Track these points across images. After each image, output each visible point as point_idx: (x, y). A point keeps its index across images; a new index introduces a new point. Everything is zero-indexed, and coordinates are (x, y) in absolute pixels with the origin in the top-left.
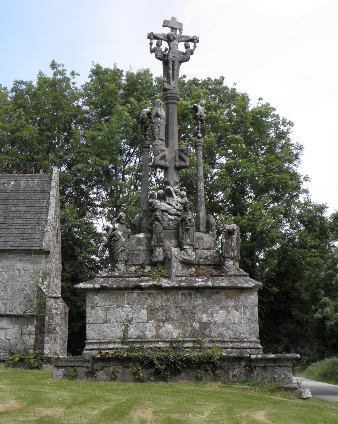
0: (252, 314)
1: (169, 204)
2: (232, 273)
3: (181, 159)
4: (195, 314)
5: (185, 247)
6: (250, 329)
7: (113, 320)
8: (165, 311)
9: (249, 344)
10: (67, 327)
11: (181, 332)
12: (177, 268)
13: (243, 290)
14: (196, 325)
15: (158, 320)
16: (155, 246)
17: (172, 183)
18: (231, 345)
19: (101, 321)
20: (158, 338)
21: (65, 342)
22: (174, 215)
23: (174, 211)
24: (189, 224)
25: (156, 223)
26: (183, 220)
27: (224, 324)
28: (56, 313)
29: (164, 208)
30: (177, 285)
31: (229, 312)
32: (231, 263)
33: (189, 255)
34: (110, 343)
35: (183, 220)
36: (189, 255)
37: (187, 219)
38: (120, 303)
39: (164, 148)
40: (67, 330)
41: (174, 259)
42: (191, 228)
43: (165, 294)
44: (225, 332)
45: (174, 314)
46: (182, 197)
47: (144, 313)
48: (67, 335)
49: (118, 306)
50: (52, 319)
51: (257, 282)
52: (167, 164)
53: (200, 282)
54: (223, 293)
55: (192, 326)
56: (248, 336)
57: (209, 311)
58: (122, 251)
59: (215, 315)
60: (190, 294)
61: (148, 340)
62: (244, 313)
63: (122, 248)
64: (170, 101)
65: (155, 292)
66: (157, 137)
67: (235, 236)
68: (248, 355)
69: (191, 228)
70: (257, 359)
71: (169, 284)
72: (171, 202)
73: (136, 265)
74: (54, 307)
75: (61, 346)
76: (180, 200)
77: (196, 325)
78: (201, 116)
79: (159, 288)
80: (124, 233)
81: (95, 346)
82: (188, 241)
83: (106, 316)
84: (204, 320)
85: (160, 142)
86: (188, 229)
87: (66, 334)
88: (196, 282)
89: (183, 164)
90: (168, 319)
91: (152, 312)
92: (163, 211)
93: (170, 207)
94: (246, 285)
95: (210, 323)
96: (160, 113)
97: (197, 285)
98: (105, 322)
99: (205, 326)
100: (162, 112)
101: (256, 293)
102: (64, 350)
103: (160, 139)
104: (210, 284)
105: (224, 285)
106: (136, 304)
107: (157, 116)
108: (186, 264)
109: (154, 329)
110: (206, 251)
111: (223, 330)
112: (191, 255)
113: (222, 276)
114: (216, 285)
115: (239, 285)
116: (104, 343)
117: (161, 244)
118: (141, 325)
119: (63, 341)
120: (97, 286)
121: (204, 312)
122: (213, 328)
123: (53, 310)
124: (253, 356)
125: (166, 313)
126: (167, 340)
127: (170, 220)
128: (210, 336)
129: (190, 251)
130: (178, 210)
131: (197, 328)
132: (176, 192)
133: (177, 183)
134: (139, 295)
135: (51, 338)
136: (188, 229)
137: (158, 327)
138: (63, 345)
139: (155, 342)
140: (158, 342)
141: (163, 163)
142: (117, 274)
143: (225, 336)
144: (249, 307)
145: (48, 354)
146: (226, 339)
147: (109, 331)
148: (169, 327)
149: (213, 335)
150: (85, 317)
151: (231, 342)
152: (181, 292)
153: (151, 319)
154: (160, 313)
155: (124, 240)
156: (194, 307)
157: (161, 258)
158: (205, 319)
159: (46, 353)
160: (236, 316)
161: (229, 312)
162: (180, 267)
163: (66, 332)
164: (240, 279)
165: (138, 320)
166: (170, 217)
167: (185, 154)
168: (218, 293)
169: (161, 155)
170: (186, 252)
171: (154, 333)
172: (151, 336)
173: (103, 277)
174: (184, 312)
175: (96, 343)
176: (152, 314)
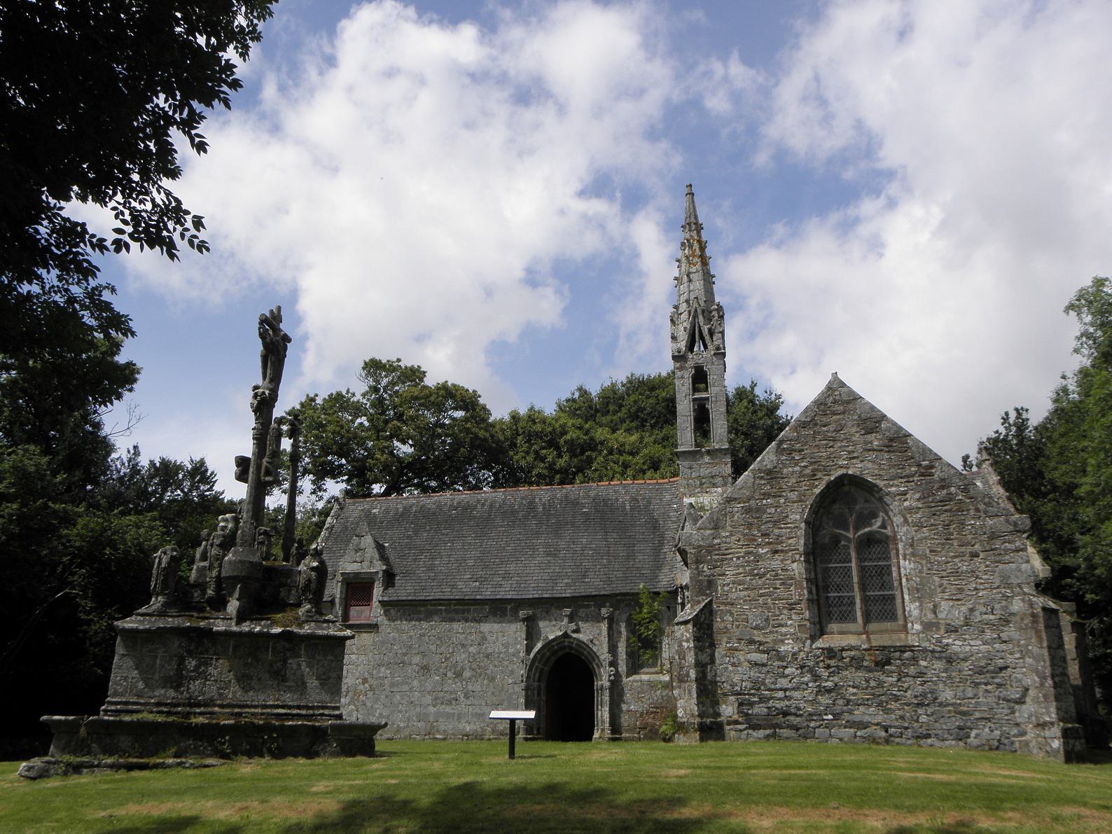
10: (1045, 644)
21: (1045, 678)
28: (688, 647)
40: (1045, 652)
48: (1048, 663)
50: (684, 658)
74: (685, 638)
75: (1037, 687)
87: (1044, 661)
102: (1045, 696)
119: (1039, 678)
123: (684, 643)
135: (685, 691)
138: (1042, 684)
145: (682, 717)
159: (680, 715)
163: (1043, 655)
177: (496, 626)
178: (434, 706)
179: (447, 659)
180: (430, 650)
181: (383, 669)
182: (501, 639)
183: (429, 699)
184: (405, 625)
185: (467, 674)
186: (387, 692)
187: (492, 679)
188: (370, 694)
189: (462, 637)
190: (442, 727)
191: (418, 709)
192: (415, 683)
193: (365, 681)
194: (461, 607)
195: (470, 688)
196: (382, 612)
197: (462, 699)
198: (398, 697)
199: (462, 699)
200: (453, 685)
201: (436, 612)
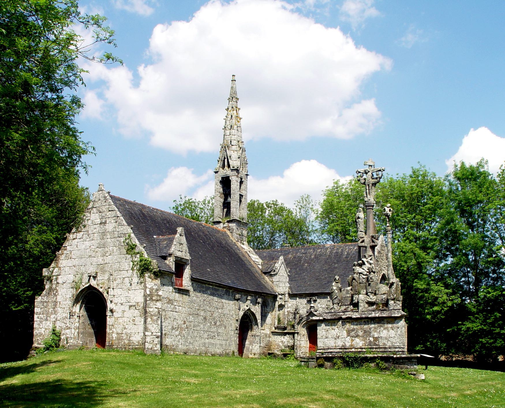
0: (401, 332)
1: (363, 269)
2: (392, 308)
3: (373, 242)
4: (371, 332)
5: (369, 294)
6: (400, 340)
7: (330, 337)
8: (355, 331)
9: (399, 349)
11: (364, 343)
12: (363, 306)
13: (396, 318)
14: (372, 339)
15: (352, 337)
16: (353, 294)
17: (367, 256)
18: (389, 350)
19: (324, 337)
20: (352, 347)
22: (366, 275)
23: (365, 273)
24: (371, 280)
25: (354, 281)
26: (368, 278)
27: (386, 338)
29: (360, 272)
30: (359, 316)
31: (388, 331)
32: (392, 302)
33: (371, 299)
34: (329, 349)
35: (368, 278)
36: (371, 299)
37: (369, 278)
38: (333, 327)
39: (364, 236)
41: (360, 301)
42: (372, 283)
43: (356, 322)
44: (386, 343)
45: (360, 333)
46: (370, 264)
47: (345, 333)
49: (332, 329)
51: (403, 313)
52: (366, 245)
53: (373, 315)
54: (385, 320)
55: (369, 339)
56: (399, 345)
57: (378, 331)
58: (335, 298)
59: (381, 333)
60: (368, 322)
61: (347, 347)
62: (397, 332)
63: (336, 296)
64: (367, 208)
65: (350, 321)
66: (359, 229)
67: (394, 286)
68: (392, 355)
69: (372, 283)
70: (397, 358)
71: (356, 316)
72: (364, 268)
73: (346, 305)
76: (369, 266)
77: (372, 339)
78: (387, 214)
79: (350, 318)
80: (338, 287)
81: (321, 351)
82: (370, 290)
83: (326, 334)
84: (375, 336)
85: (360, 233)
86: (370, 284)
88: (371, 314)
89: (374, 244)
90: (357, 336)
91: (349, 332)
92: (360, 273)
93: (363, 271)
94: (396, 315)
95: (379, 338)
96: (360, 216)
97: (370, 316)
98: (327, 338)
99: (376, 339)
100: (361, 215)
101: (403, 319)
103: (360, 231)
104: (377, 315)
105: (384, 315)
106: (341, 328)
107: (359, 218)
108: (370, 304)
109: (350, 341)
110: (383, 296)
111: (385, 341)
112: (373, 298)
113: (386, 310)
114: (380, 316)
115: (393, 315)
116: (326, 349)
117: (356, 293)
118: (343, 339)
120: (321, 318)
121: (375, 332)
122: (380, 340)
124: (395, 356)
125: (356, 332)
126: (356, 347)
127: (364, 278)
128: (379, 345)
129: (371, 296)
130: (367, 272)
131: (372, 341)
132: (367, 262)
133: (371, 256)
134: (342, 322)
136: (370, 284)
137: (352, 340)
139: (350, 348)
140: (352, 348)
141: (363, 244)
142: (333, 311)
143: (386, 345)
144: (400, 328)
146: (387, 347)
147: (328, 342)
148: (357, 340)
149: (381, 344)
150: (317, 335)
151: (390, 348)
152: (363, 320)
153: (348, 336)
154: (353, 333)
155: (336, 291)
156: (370, 329)
157: (356, 301)
158: (376, 335)
160: (392, 333)
161: (388, 331)
162: (366, 305)
164: (396, 312)
165: (342, 337)
166: (364, 276)
167: (375, 238)
168: (383, 320)
169: (361, 240)
170: (369, 297)
171: (350, 344)
172: (348, 345)
173: (326, 313)
174: (365, 332)
175: (322, 349)
176: (349, 333)
177: (227, 301)
178: (208, 339)
179: (212, 314)
180: (207, 309)
181: (191, 316)
182: (228, 307)
183: (206, 336)
184: (199, 294)
185: (218, 323)
186: (192, 330)
187: (225, 327)
188: (186, 329)
189: (217, 303)
190: (210, 351)
191: (203, 340)
192: (202, 326)
193: (185, 323)
194: (217, 288)
195: (219, 331)
196: (191, 284)
197: (216, 336)
198: (196, 333)
199: (216, 336)
200: (214, 330)
201: (208, 289)
